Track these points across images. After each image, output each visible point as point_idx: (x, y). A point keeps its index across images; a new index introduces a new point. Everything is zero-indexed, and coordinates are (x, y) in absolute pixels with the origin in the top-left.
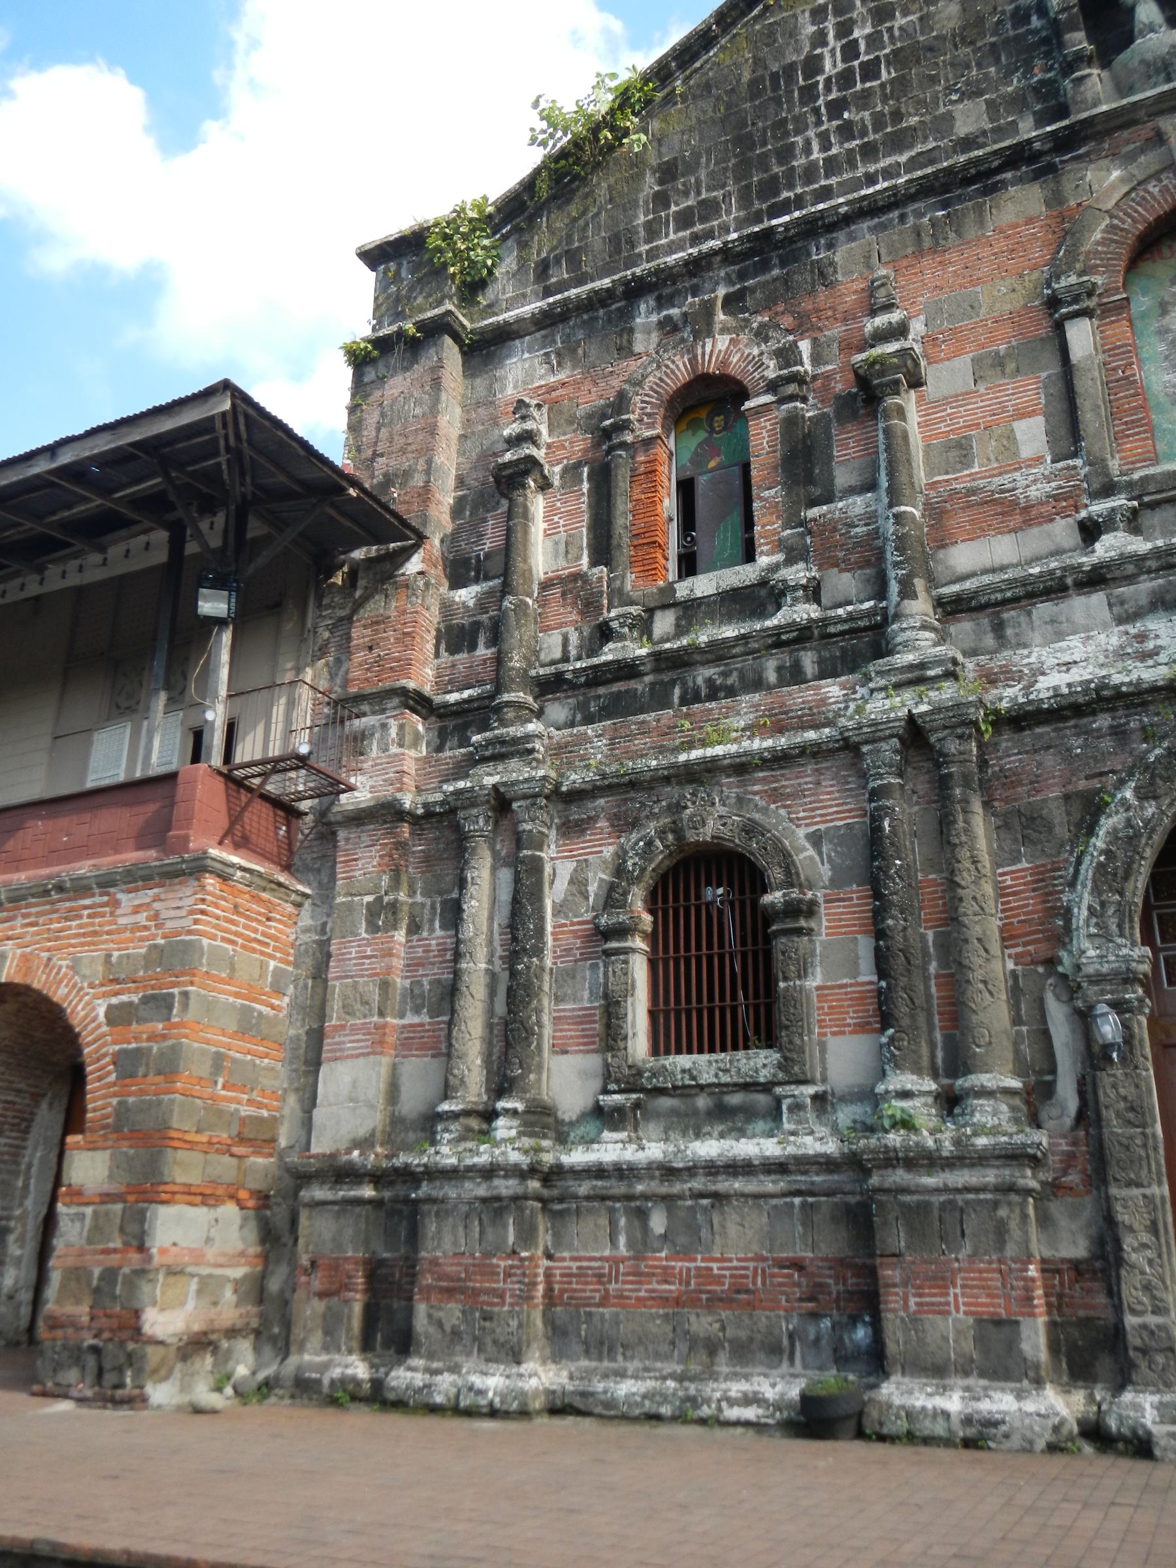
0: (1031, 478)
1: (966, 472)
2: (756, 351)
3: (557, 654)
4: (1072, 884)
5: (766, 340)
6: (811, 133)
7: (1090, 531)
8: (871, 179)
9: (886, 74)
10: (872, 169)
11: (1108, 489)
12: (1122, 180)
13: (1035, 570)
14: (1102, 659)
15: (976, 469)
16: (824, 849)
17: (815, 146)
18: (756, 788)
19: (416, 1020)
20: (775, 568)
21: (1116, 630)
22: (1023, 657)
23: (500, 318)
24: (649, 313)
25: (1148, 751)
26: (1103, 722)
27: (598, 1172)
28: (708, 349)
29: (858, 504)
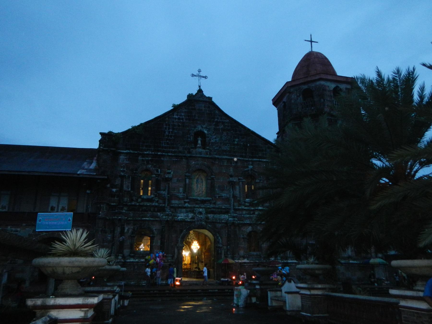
2: (154, 169)
3: (126, 201)
5: (155, 168)
6: (163, 142)
7: (185, 202)
8: (169, 152)
9: (173, 138)
10: (170, 150)
11: (187, 198)
15: (175, 192)
17: (164, 144)
19: (106, 244)
20: (153, 197)
23: (121, 151)
26: (184, 223)
27: (130, 262)
29: (162, 192)
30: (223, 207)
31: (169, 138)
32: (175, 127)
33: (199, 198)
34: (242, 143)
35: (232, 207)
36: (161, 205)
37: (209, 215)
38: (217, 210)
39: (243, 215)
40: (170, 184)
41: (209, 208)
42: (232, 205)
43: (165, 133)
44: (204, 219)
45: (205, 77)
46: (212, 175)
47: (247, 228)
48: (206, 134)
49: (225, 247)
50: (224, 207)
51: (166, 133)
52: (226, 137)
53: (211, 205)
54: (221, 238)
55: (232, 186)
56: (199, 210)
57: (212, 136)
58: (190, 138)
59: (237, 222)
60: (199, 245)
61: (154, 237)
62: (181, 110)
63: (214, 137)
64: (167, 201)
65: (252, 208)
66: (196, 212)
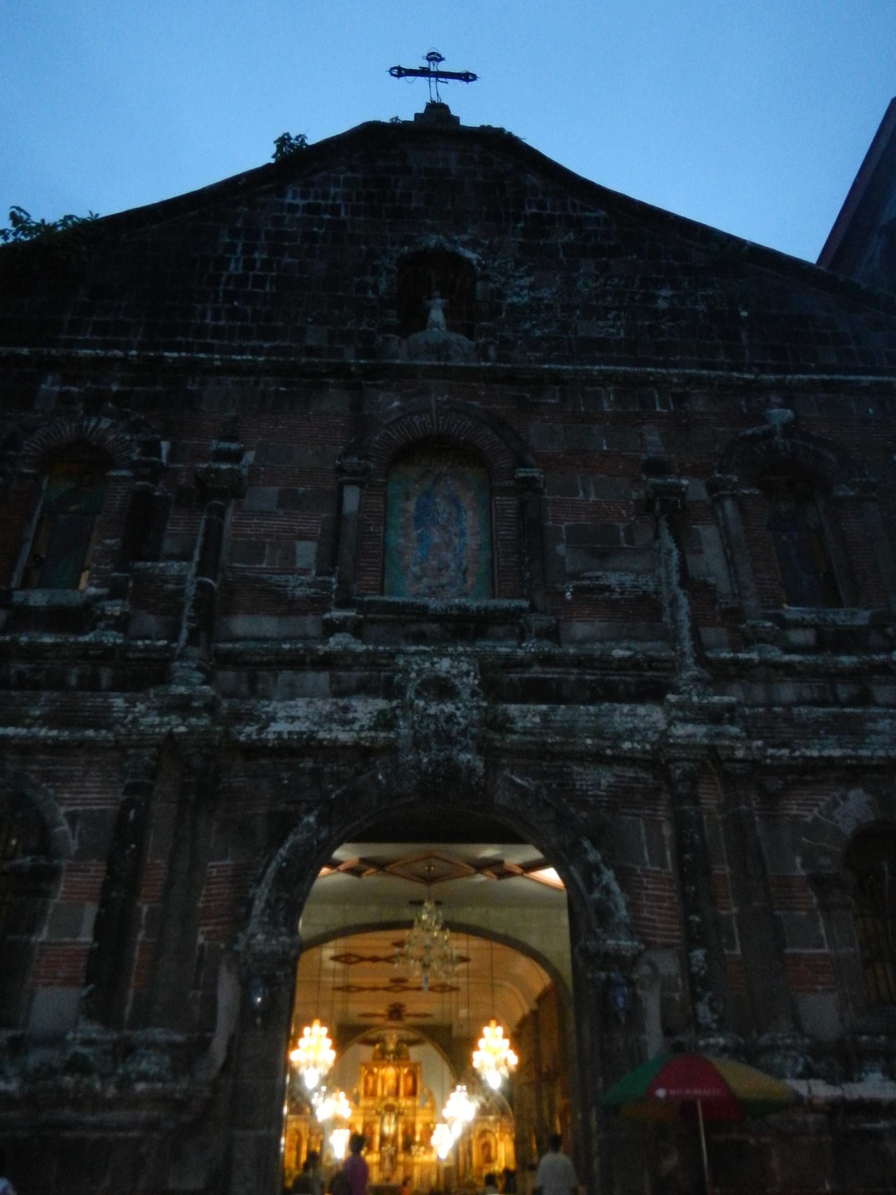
0: (299, 582)
1: (257, 566)
2: (128, 438)
4: (258, 882)
7: (331, 628)
8: (241, 351)
10: (245, 344)
12: (399, 408)
13: (286, 646)
14: (316, 719)
15: (264, 566)
16: (78, 827)
17: (209, 314)
18: (35, 767)
20: (97, 598)
21: (330, 700)
22: (264, 706)
24: (53, 384)
25: (332, 791)
26: (308, 764)
28: (92, 424)
29: (175, 567)
30: (618, 653)
31: (249, 288)
32: (286, 244)
33: (434, 604)
34: (701, 307)
35: (687, 645)
36: (140, 643)
37: (513, 709)
38: (573, 675)
39: (777, 709)
40: (230, 518)
41: (509, 663)
42: (685, 632)
43: (227, 269)
44: (474, 730)
45: (467, 77)
46: (524, 464)
47: (835, 804)
48: (475, 262)
49: (668, 965)
50: (628, 653)
51: (232, 266)
52: (596, 281)
53: (524, 645)
54: (624, 877)
55: (667, 520)
56: (433, 664)
57: (512, 280)
58: (375, 288)
59: (749, 748)
60: (512, 1046)
61: (53, 874)
62: (324, 173)
63: (527, 281)
64: (187, 611)
65: (846, 660)
66: (409, 680)
